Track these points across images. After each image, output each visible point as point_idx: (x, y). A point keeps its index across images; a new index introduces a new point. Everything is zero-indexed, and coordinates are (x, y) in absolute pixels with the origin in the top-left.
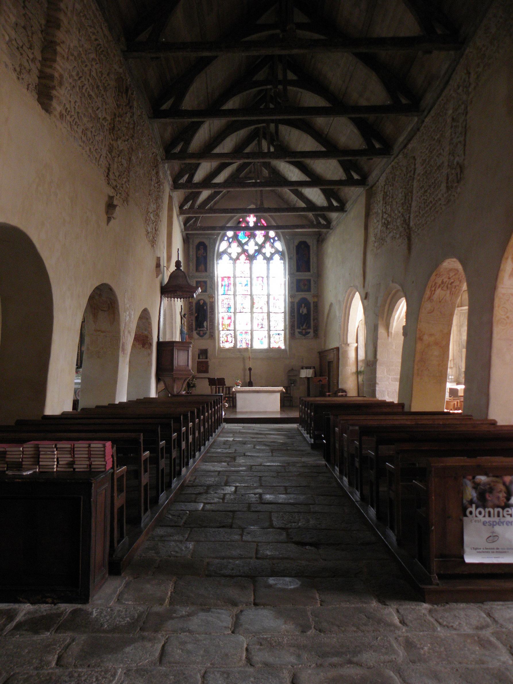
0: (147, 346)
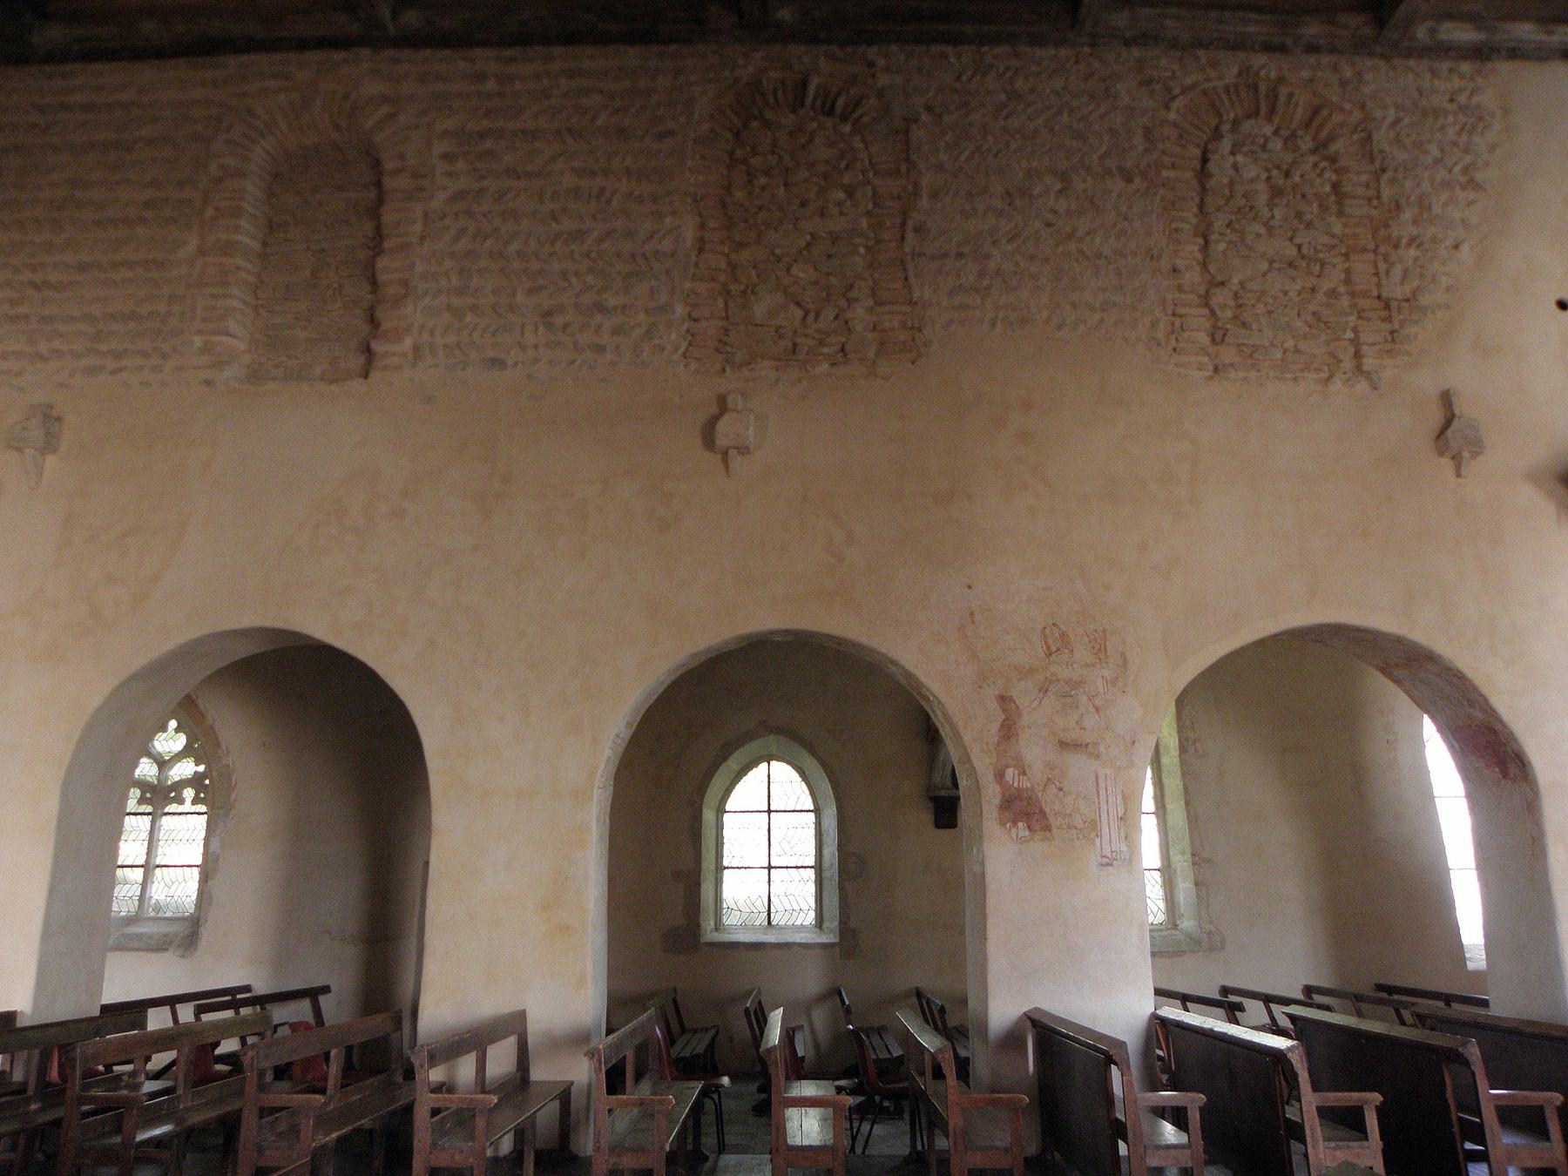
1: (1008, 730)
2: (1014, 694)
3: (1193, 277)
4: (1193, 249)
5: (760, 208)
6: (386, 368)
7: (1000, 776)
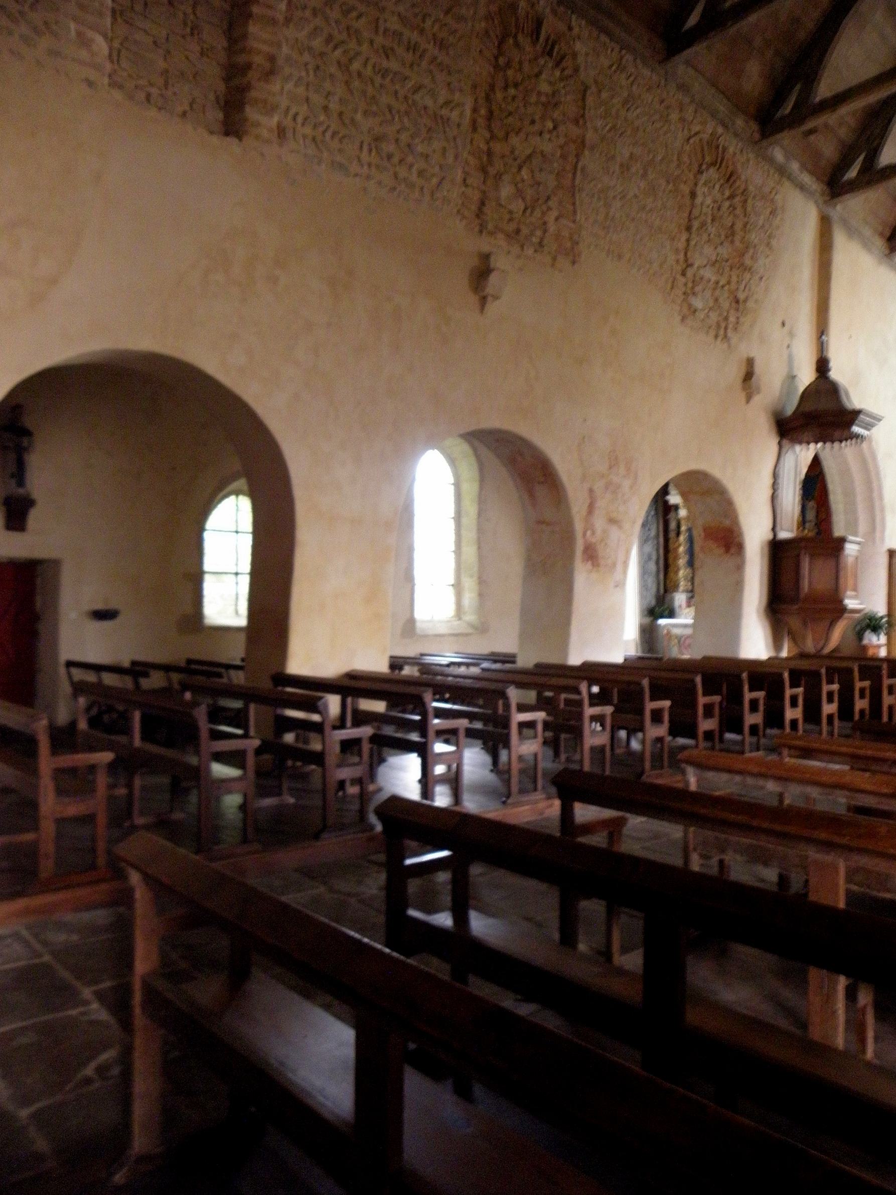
0: (733, 550)
3: (682, 256)
5: (510, 114)
6: (257, 137)
7: (584, 534)
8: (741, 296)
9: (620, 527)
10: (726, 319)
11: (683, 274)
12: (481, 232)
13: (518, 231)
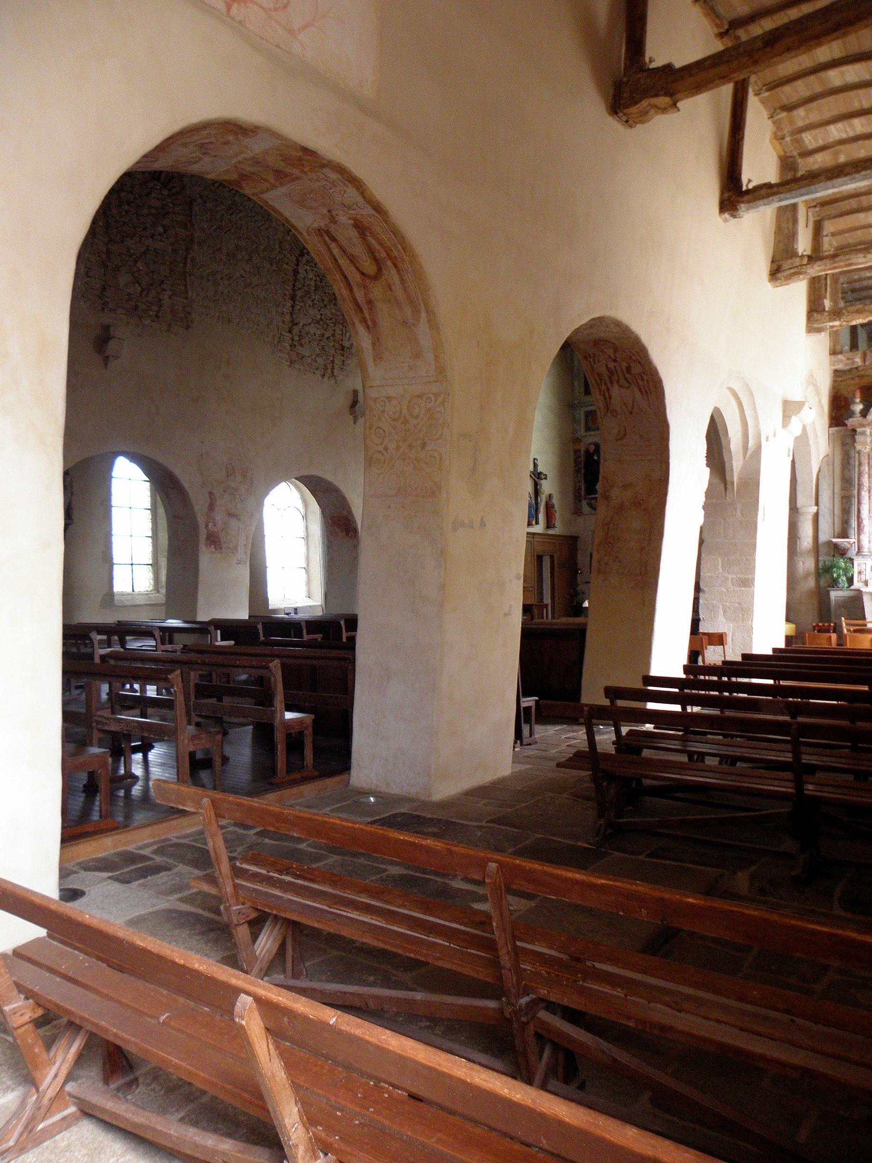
0: (351, 533)
1: (211, 507)
2: (215, 492)
3: (288, 318)
4: (289, 303)
5: (124, 224)
7: (207, 526)
8: (346, 344)
9: (239, 520)
10: (333, 362)
11: (290, 331)
12: (103, 309)
13: (136, 307)
